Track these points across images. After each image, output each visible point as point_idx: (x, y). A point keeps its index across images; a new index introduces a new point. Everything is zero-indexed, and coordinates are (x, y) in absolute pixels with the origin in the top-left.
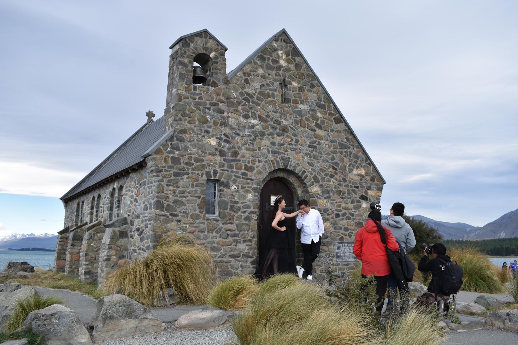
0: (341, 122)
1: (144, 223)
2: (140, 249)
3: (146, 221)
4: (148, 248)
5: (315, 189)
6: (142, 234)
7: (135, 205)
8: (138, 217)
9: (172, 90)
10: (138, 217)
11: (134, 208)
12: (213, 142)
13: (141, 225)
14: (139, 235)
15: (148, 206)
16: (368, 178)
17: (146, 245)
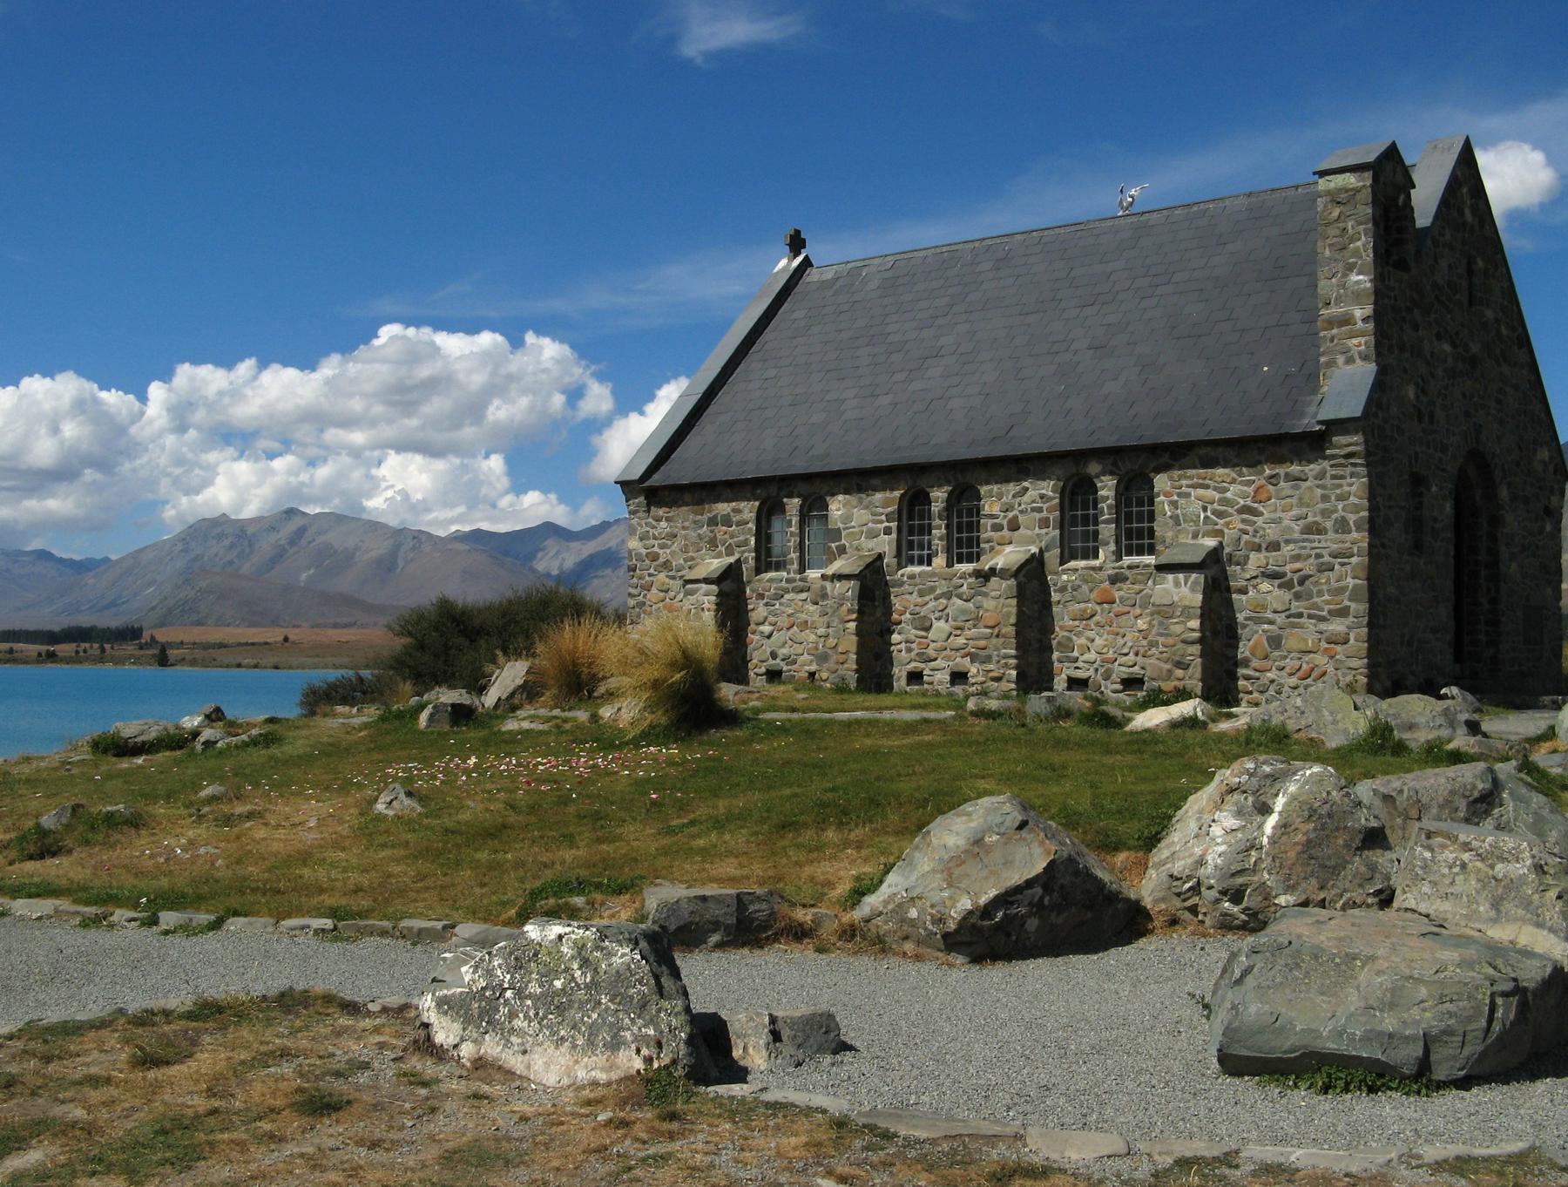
0: (1521, 346)
1: (1312, 560)
2: (1300, 615)
3: (1318, 556)
4: (1343, 613)
5: (1504, 493)
6: (1301, 582)
7: (1243, 521)
8: (1274, 546)
9: (1345, 275)
10: (1274, 546)
11: (1242, 526)
12: (1411, 392)
13: (1298, 565)
14: (1287, 585)
15: (1329, 524)
16: (1551, 468)
17: (1327, 607)
